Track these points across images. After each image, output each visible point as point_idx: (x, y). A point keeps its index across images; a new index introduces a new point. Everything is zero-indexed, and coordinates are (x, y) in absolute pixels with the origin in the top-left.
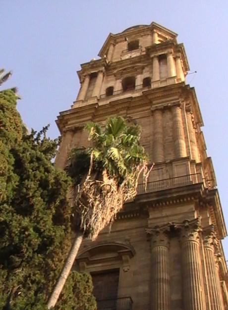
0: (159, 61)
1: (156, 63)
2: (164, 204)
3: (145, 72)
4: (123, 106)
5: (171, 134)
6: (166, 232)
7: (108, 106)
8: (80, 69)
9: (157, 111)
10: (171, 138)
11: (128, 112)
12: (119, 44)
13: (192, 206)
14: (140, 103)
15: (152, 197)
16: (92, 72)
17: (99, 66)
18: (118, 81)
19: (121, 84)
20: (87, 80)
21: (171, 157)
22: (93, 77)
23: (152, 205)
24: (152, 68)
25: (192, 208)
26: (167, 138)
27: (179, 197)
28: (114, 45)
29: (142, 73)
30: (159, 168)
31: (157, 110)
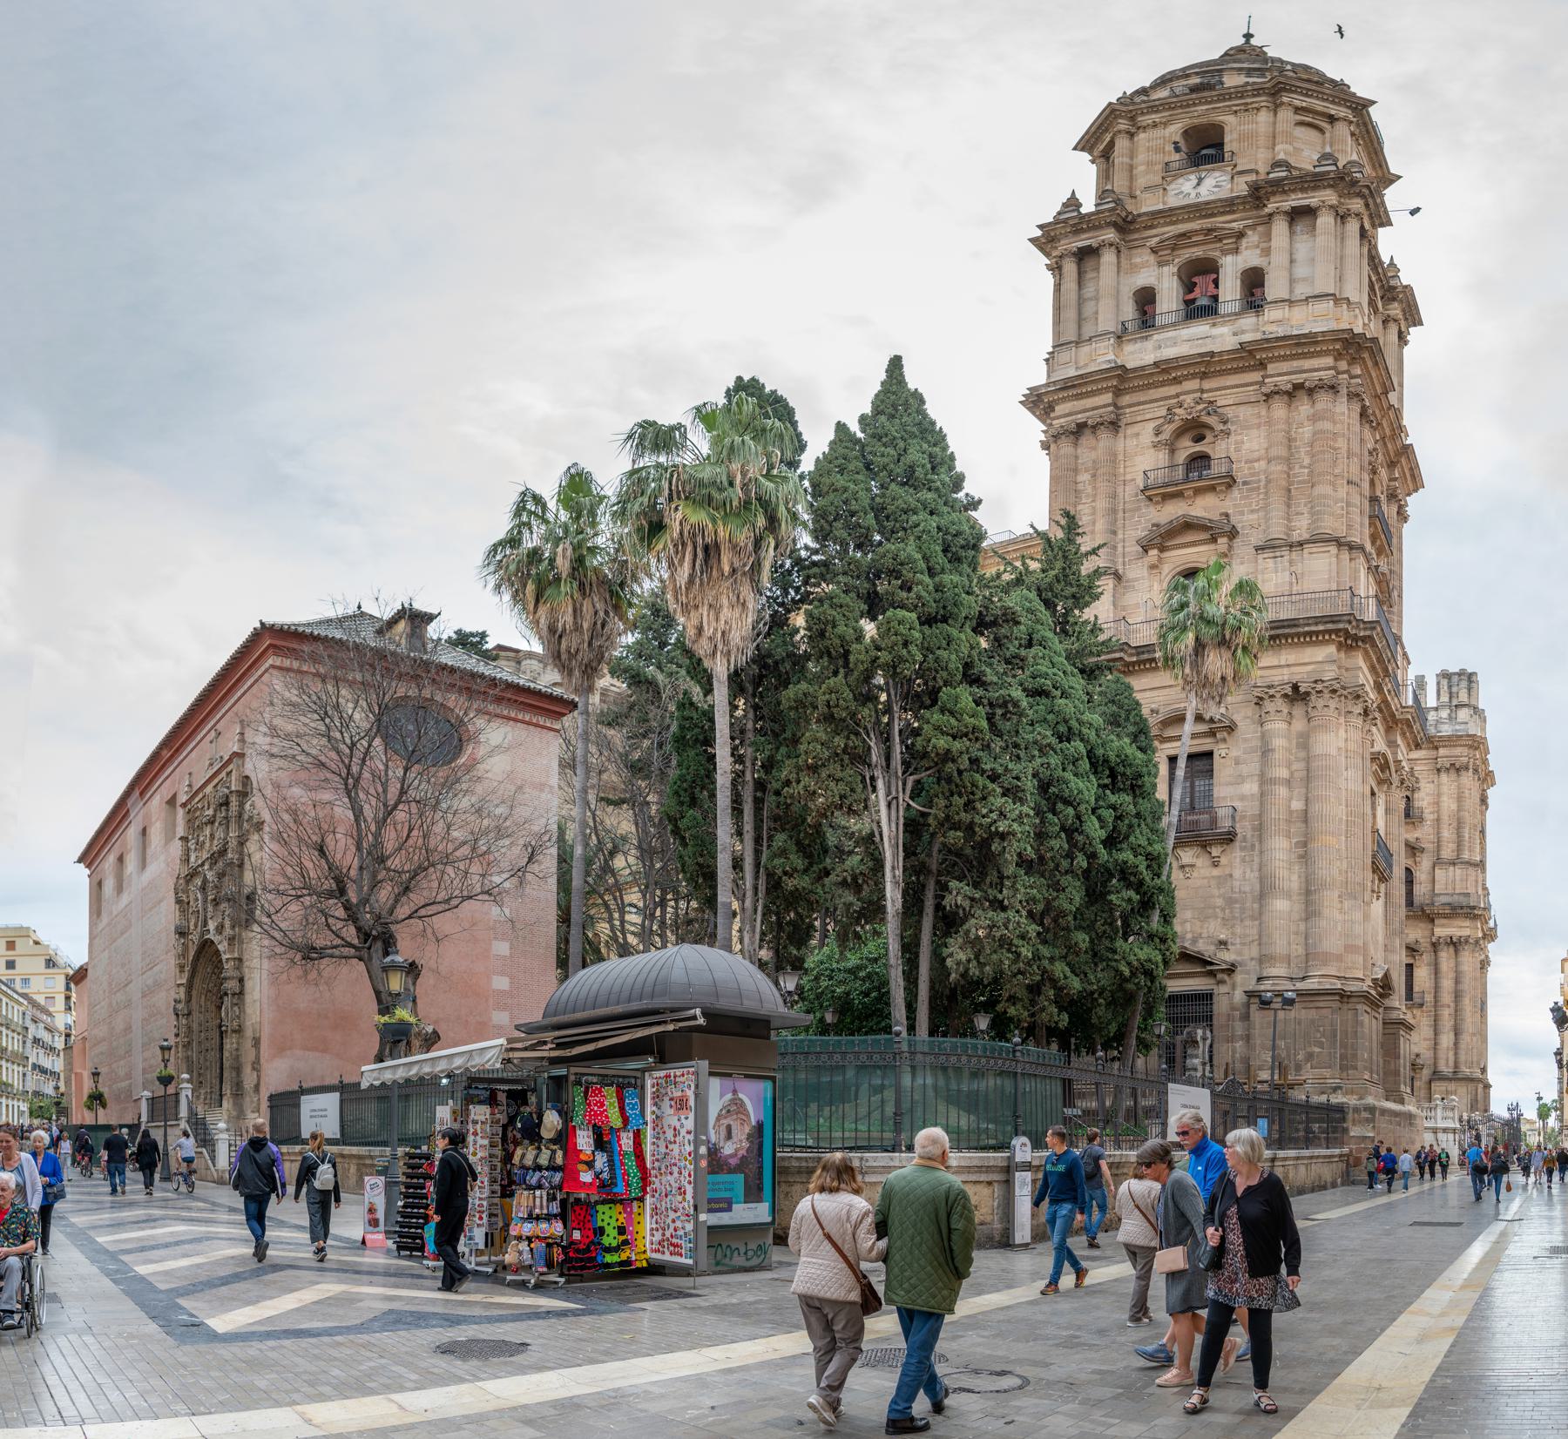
5: (1307, 461)
11: (1207, 385)
26: (1297, 470)
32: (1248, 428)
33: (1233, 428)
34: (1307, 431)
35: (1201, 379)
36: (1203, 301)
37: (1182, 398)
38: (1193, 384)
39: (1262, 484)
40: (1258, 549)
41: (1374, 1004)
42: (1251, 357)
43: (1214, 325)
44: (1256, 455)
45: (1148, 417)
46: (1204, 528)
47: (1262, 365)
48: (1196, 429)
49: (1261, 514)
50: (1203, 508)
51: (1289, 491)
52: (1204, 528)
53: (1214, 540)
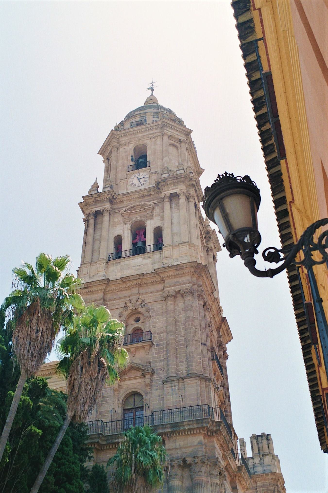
2: (177, 434)
3: (155, 217)
4: (135, 282)
5: (183, 334)
6: (179, 466)
7: (119, 281)
9: (169, 298)
10: (183, 338)
12: (124, 147)
14: (152, 280)
15: (167, 428)
16: (97, 209)
17: (102, 201)
18: (126, 226)
19: (130, 231)
20: (92, 222)
21: (183, 372)
22: (98, 214)
23: (168, 435)
25: (201, 440)
26: (180, 338)
27: (190, 430)
28: (117, 149)
29: (152, 218)
30: (173, 384)
33: (152, 315)
34: (182, 317)
36: (140, 244)
37: (131, 297)
38: (135, 290)
39: (165, 345)
43: (144, 259)
44: (161, 330)
45: (117, 307)
46: (139, 369)
49: (165, 362)
51: (177, 349)
52: (139, 369)
53: (144, 376)
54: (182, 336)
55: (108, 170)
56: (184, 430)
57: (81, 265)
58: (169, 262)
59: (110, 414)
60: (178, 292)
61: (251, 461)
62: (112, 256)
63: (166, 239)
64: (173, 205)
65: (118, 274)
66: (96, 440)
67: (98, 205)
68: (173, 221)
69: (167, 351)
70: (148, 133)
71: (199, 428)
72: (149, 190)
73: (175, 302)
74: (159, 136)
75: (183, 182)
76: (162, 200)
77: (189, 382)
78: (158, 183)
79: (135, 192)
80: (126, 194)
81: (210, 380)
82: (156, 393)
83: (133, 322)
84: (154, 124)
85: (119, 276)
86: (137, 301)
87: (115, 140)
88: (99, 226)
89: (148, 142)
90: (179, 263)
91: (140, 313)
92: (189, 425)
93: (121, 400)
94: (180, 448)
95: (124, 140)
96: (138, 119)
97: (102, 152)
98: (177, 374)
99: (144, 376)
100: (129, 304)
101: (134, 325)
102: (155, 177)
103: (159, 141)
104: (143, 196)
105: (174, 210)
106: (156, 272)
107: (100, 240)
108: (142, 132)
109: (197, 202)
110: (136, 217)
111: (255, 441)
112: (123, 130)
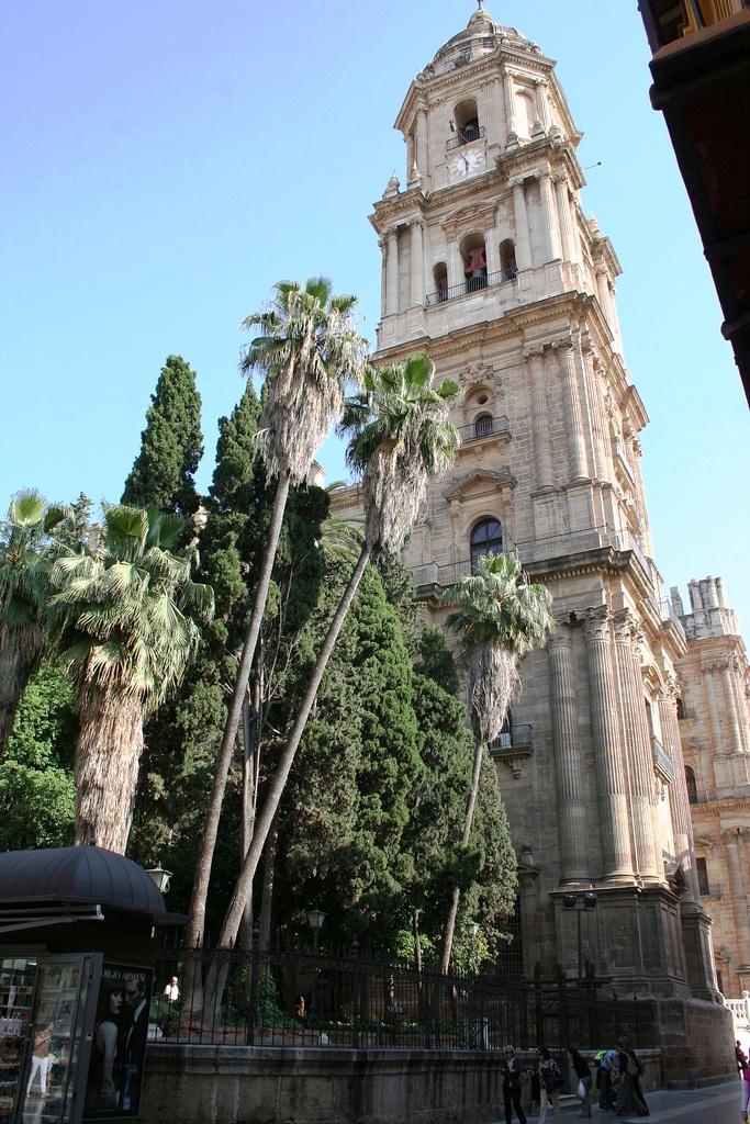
0: (525, 192)
1: (519, 195)
4: (474, 338)
5: (560, 416)
8: (373, 211)
9: (533, 358)
11: (486, 351)
13: (600, 579)
14: (502, 331)
15: (542, 568)
16: (400, 222)
17: (407, 207)
20: (393, 245)
21: (564, 480)
22: (402, 231)
24: (512, 207)
27: (580, 568)
28: (426, 113)
30: (548, 499)
31: (532, 355)
32: (517, 388)
33: (506, 389)
34: (557, 387)
35: (481, 346)
38: (475, 352)
40: (533, 496)
41: (671, 901)
42: (513, 323)
43: (486, 296)
46: (492, 480)
47: (520, 331)
48: (479, 393)
50: (490, 461)
52: (492, 480)
53: (499, 490)
54: (558, 420)
55: (413, 155)
56: (570, 570)
57: (382, 319)
58: (529, 298)
59: (448, 554)
60: (547, 348)
61: (690, 620)
62: (433, 299)
63: (523, 259)
64: (530, 198)
65: (444, 328)
66: (429, 594)
67: (401, 215)
68: (531, 227)
69: (535, 446)
70: (476, 77)
71: (595, 565)
72: (487, 177)
73: (543, 364)
74: (497, 81)
75: (544, 155)
76: (510, 193)
77: (575, 493)
78: (500, 164)
79: (463, 184)
80: (446, 190)
81: (608, 487)
82: (520, 515)
83: (476, 405)
84: (486, 60)
85: (445, 330)
86: (480, 369)
87: (420, 99)
88: (405, 252)
89: (477, 94)
90: (547, 297)
91: (486, 389)
92: (577, 560)
93: (464, 531)
94: (566, 597)
95: (434, 96)
96: (457, 54)
97: (400, 125)
98: (556, 482)
99: (499, 490)
100: (467, 376)
101: (476, 409)
102: (495, 153)
103: (497, 88)
104: (476, 191)
105: (533, 207)
106: (509, 318)
107: (410, 274)
108: (466, 77)
109: (572, 190)
110: (467, 229)
111: (696, 591)
112: (432, 79)
